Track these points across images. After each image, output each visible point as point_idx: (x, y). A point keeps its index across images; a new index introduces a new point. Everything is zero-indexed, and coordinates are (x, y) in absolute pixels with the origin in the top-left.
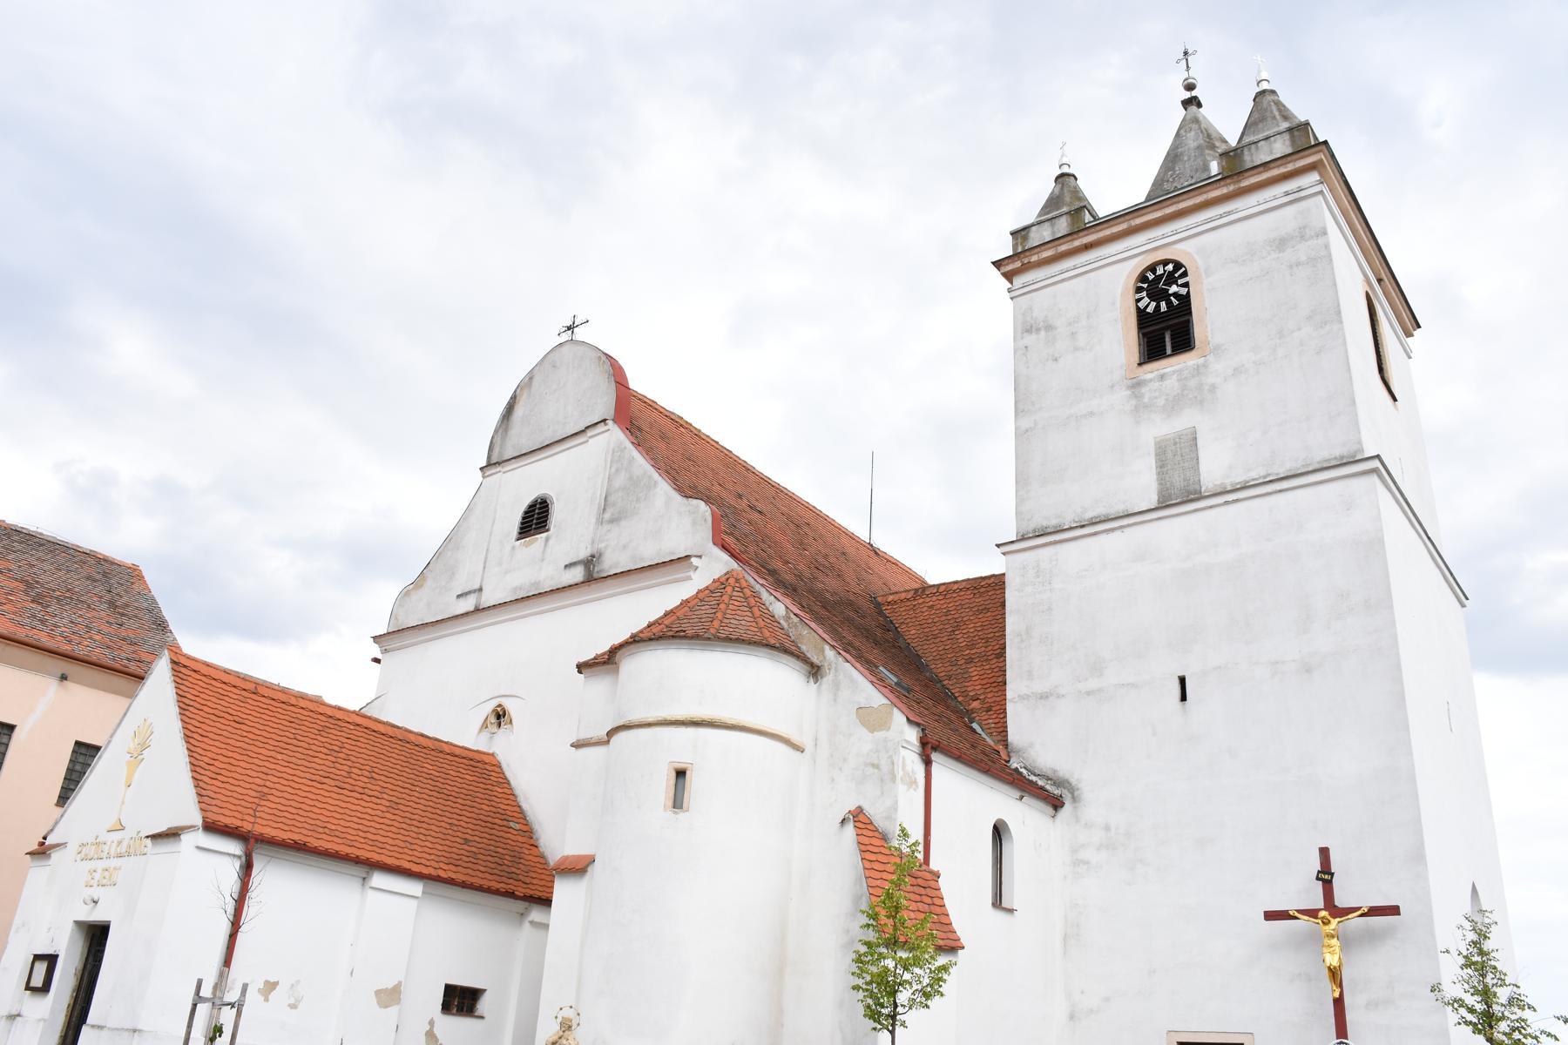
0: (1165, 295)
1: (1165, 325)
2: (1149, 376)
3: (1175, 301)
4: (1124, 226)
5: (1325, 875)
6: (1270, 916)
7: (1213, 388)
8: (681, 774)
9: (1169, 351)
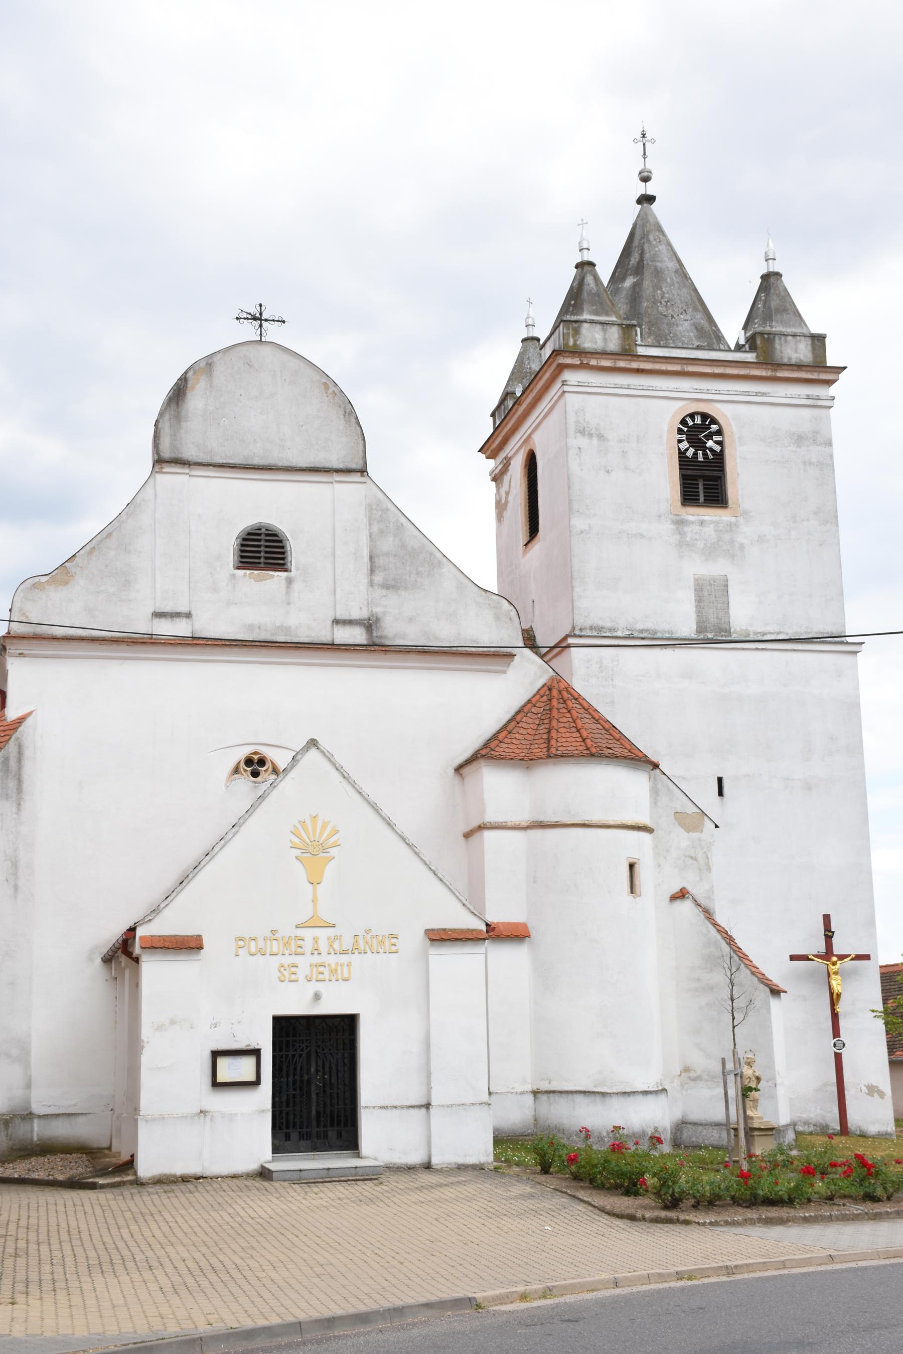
0: (704, 448)
1: (703, 479)
2: (691, 518)
4: (677, 368)
5: (829, 935)
6: (793, 958)
7: (742, 547)
8: (632, 866)
9: (702, 499)
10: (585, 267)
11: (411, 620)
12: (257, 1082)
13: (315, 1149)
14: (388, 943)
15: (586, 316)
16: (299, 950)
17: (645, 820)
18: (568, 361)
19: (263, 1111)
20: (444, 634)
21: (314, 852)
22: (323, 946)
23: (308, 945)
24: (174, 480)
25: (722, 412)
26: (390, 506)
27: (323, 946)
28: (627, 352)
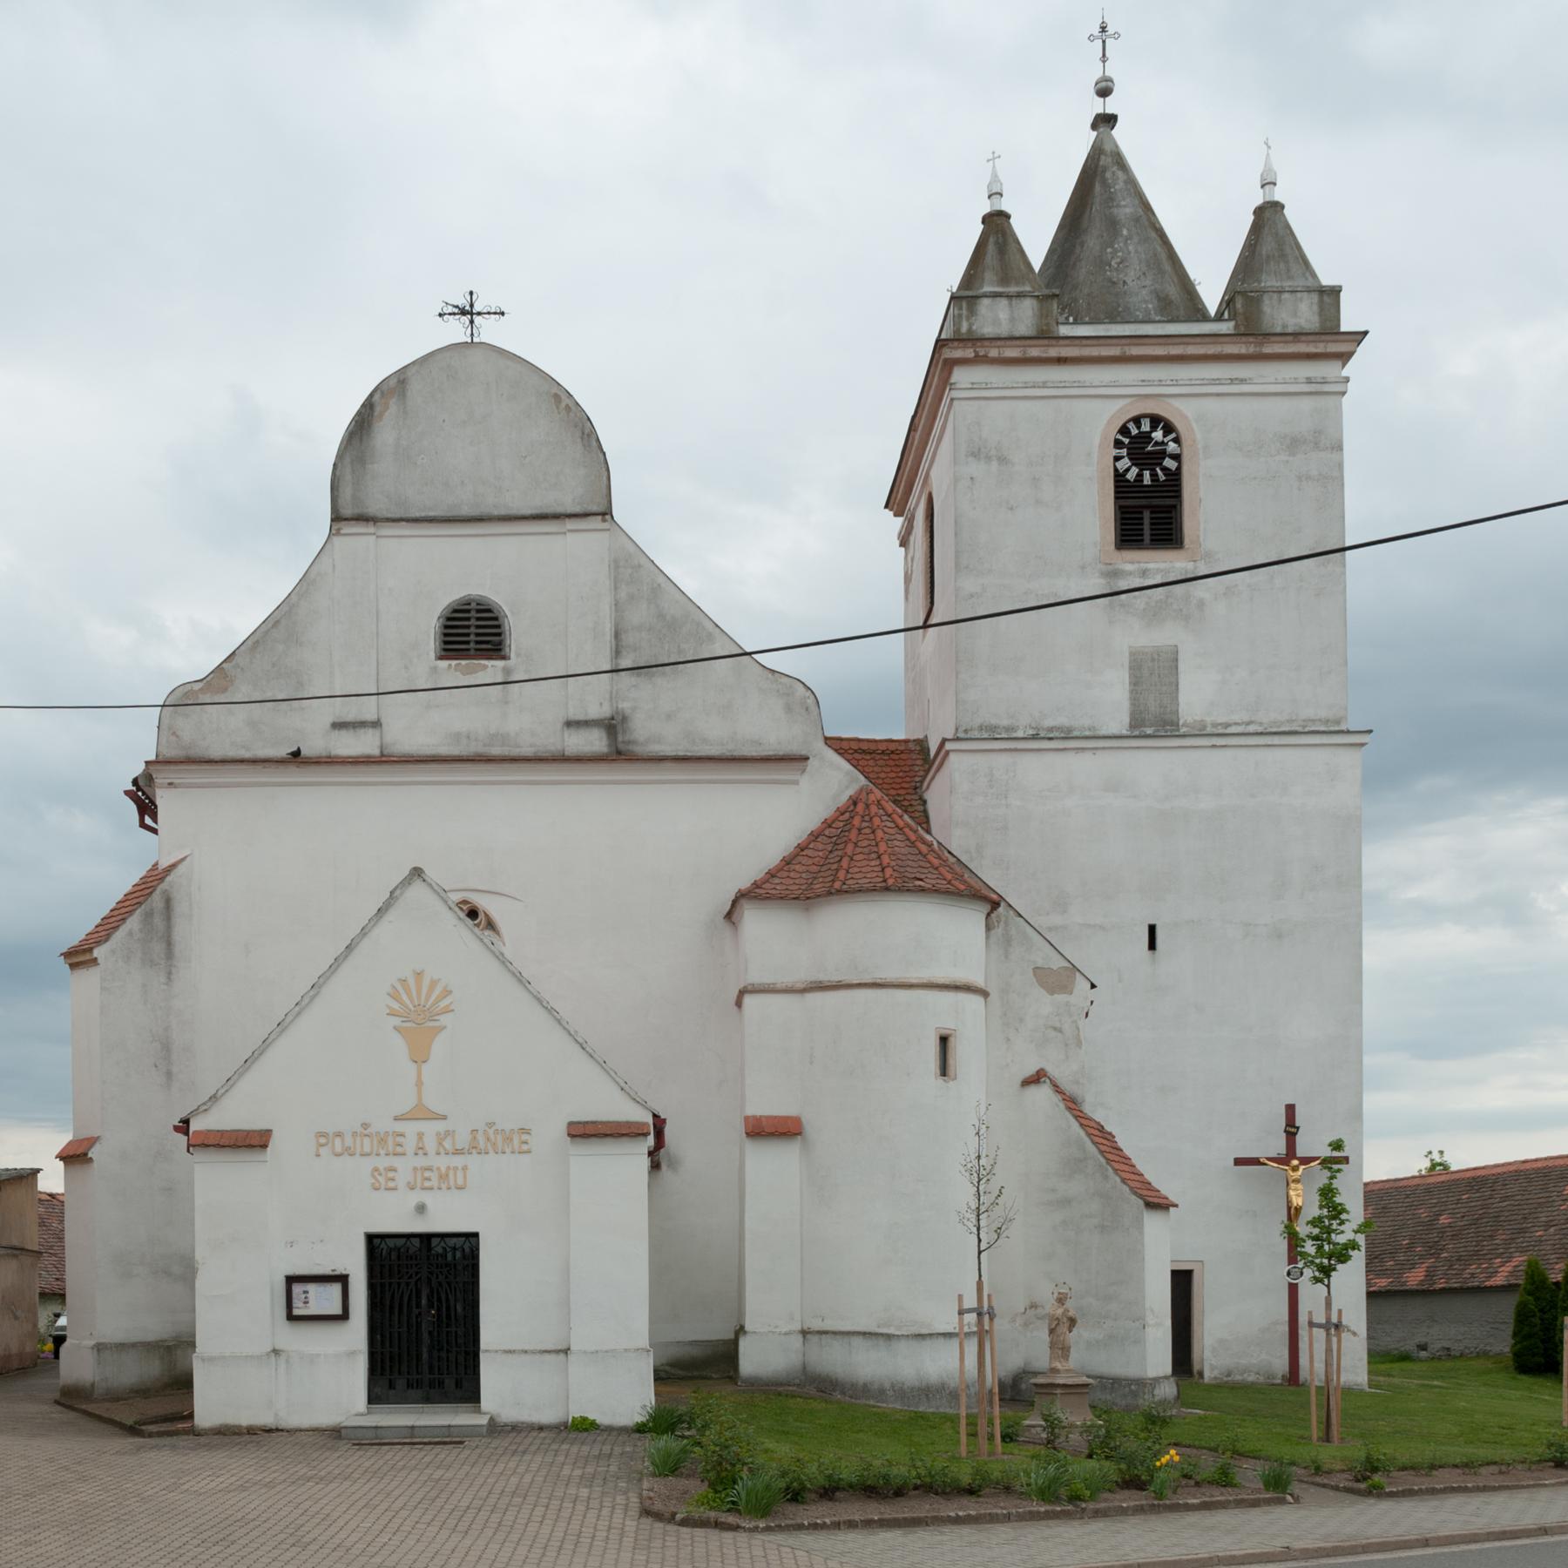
1: (1149, 505)
3: (1162, 477)
8: (944, 1040)
10: (997, 224)
11: (669, 717)
12: (344, 1316)
13: (428, 1400)
14: (514, 1140)
15: (987, 289)
16: (399, 1149)
17: (978, 980)
18: (958, 354)
19: (352, 1354)
20: (715, 735)
21: (419, 1020)
22: (430, 1144)
23: (410, 1144)
24: (359, 541)
25: (1182, 412)
26: (643, 561)
27: (430, 1144)
28: (1044, 335)
